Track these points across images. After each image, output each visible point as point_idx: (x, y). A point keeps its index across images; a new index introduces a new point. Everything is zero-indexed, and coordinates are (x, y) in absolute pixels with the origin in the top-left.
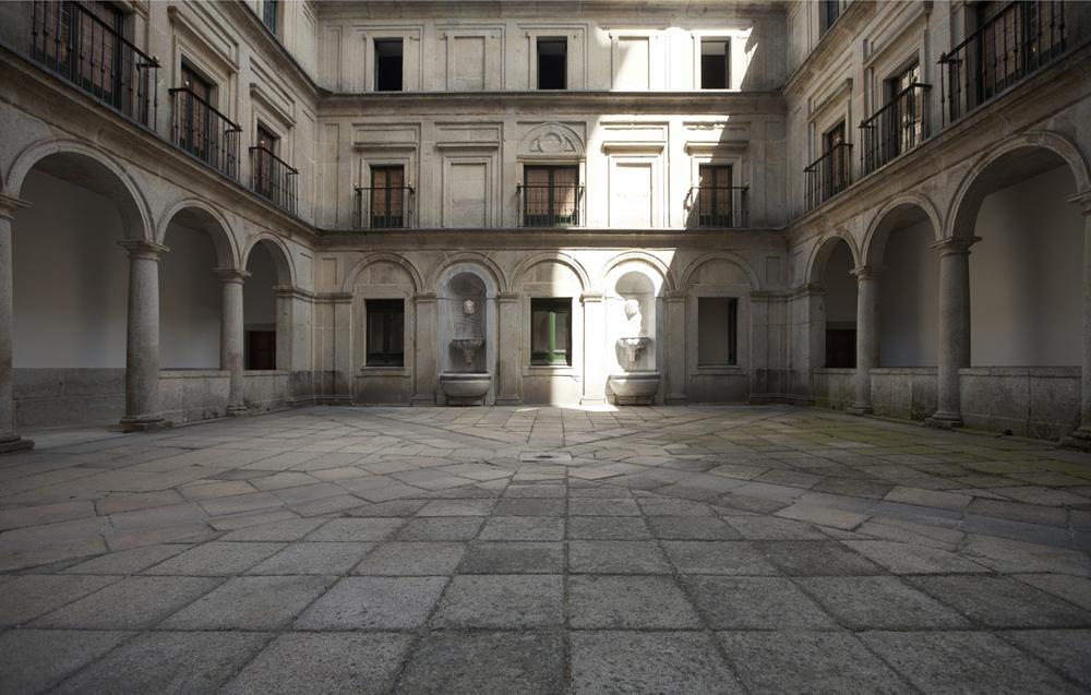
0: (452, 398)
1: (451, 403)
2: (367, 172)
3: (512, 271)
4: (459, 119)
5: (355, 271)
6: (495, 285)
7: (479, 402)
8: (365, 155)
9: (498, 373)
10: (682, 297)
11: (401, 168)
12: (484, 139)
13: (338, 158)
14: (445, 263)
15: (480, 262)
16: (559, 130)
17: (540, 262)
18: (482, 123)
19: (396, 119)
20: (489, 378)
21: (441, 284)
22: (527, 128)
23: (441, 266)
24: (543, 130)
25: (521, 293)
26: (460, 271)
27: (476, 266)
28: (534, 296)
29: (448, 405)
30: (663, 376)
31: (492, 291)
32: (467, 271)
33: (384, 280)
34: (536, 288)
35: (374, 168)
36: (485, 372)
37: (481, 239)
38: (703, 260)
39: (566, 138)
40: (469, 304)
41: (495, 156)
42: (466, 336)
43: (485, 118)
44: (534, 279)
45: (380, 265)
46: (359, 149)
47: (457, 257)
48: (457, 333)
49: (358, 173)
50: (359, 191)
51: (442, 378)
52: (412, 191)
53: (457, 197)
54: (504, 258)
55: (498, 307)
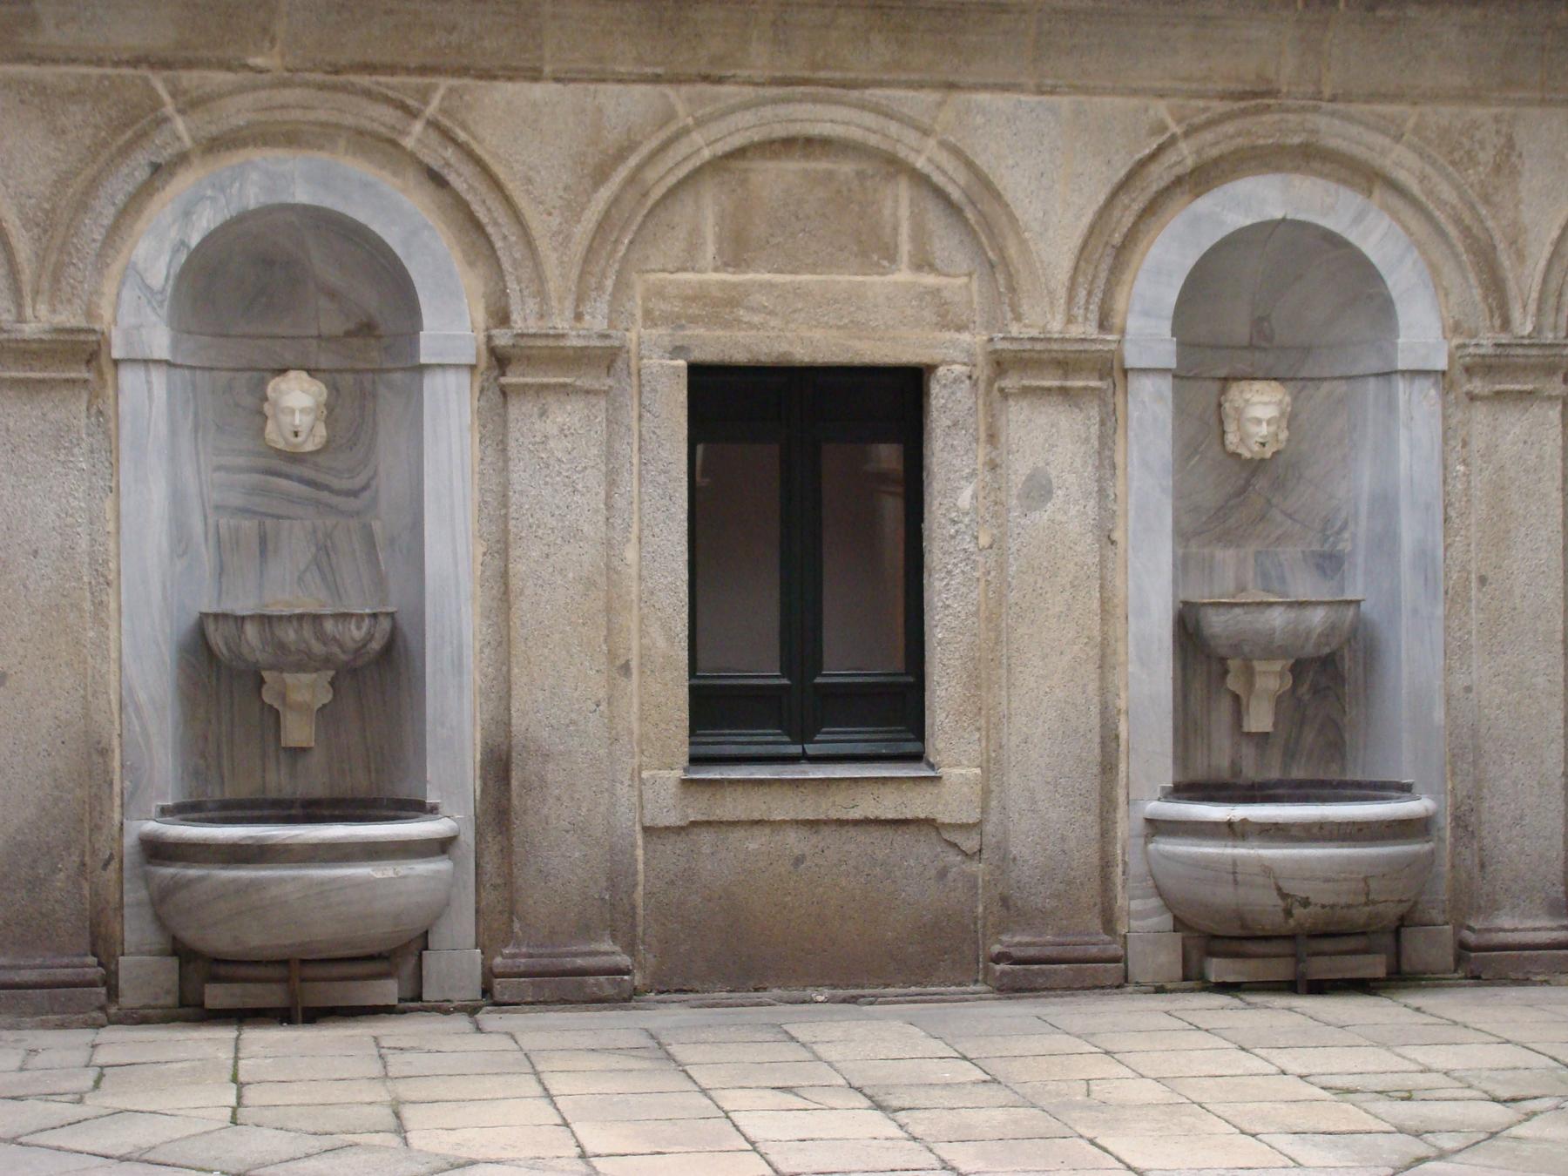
0: (219, 966)
1: (216, 995)
3: (573, 211)
7: (388, 991)
14: (160, 147)
15: (384, 148)
17: (740, 153)
20: (442, 846)
23: (136, 169)
25: (635, 335)
26: (252, 195)
28: (700, 356)
30: (1446, 822)
31: (450, 324)
32: (302, 195)
36: (417, 808)
40: (298, 399)
42: (285, 589)
44: (711, 249)
47: (238, 112)
48: (221, 570)
51: (157, 851)
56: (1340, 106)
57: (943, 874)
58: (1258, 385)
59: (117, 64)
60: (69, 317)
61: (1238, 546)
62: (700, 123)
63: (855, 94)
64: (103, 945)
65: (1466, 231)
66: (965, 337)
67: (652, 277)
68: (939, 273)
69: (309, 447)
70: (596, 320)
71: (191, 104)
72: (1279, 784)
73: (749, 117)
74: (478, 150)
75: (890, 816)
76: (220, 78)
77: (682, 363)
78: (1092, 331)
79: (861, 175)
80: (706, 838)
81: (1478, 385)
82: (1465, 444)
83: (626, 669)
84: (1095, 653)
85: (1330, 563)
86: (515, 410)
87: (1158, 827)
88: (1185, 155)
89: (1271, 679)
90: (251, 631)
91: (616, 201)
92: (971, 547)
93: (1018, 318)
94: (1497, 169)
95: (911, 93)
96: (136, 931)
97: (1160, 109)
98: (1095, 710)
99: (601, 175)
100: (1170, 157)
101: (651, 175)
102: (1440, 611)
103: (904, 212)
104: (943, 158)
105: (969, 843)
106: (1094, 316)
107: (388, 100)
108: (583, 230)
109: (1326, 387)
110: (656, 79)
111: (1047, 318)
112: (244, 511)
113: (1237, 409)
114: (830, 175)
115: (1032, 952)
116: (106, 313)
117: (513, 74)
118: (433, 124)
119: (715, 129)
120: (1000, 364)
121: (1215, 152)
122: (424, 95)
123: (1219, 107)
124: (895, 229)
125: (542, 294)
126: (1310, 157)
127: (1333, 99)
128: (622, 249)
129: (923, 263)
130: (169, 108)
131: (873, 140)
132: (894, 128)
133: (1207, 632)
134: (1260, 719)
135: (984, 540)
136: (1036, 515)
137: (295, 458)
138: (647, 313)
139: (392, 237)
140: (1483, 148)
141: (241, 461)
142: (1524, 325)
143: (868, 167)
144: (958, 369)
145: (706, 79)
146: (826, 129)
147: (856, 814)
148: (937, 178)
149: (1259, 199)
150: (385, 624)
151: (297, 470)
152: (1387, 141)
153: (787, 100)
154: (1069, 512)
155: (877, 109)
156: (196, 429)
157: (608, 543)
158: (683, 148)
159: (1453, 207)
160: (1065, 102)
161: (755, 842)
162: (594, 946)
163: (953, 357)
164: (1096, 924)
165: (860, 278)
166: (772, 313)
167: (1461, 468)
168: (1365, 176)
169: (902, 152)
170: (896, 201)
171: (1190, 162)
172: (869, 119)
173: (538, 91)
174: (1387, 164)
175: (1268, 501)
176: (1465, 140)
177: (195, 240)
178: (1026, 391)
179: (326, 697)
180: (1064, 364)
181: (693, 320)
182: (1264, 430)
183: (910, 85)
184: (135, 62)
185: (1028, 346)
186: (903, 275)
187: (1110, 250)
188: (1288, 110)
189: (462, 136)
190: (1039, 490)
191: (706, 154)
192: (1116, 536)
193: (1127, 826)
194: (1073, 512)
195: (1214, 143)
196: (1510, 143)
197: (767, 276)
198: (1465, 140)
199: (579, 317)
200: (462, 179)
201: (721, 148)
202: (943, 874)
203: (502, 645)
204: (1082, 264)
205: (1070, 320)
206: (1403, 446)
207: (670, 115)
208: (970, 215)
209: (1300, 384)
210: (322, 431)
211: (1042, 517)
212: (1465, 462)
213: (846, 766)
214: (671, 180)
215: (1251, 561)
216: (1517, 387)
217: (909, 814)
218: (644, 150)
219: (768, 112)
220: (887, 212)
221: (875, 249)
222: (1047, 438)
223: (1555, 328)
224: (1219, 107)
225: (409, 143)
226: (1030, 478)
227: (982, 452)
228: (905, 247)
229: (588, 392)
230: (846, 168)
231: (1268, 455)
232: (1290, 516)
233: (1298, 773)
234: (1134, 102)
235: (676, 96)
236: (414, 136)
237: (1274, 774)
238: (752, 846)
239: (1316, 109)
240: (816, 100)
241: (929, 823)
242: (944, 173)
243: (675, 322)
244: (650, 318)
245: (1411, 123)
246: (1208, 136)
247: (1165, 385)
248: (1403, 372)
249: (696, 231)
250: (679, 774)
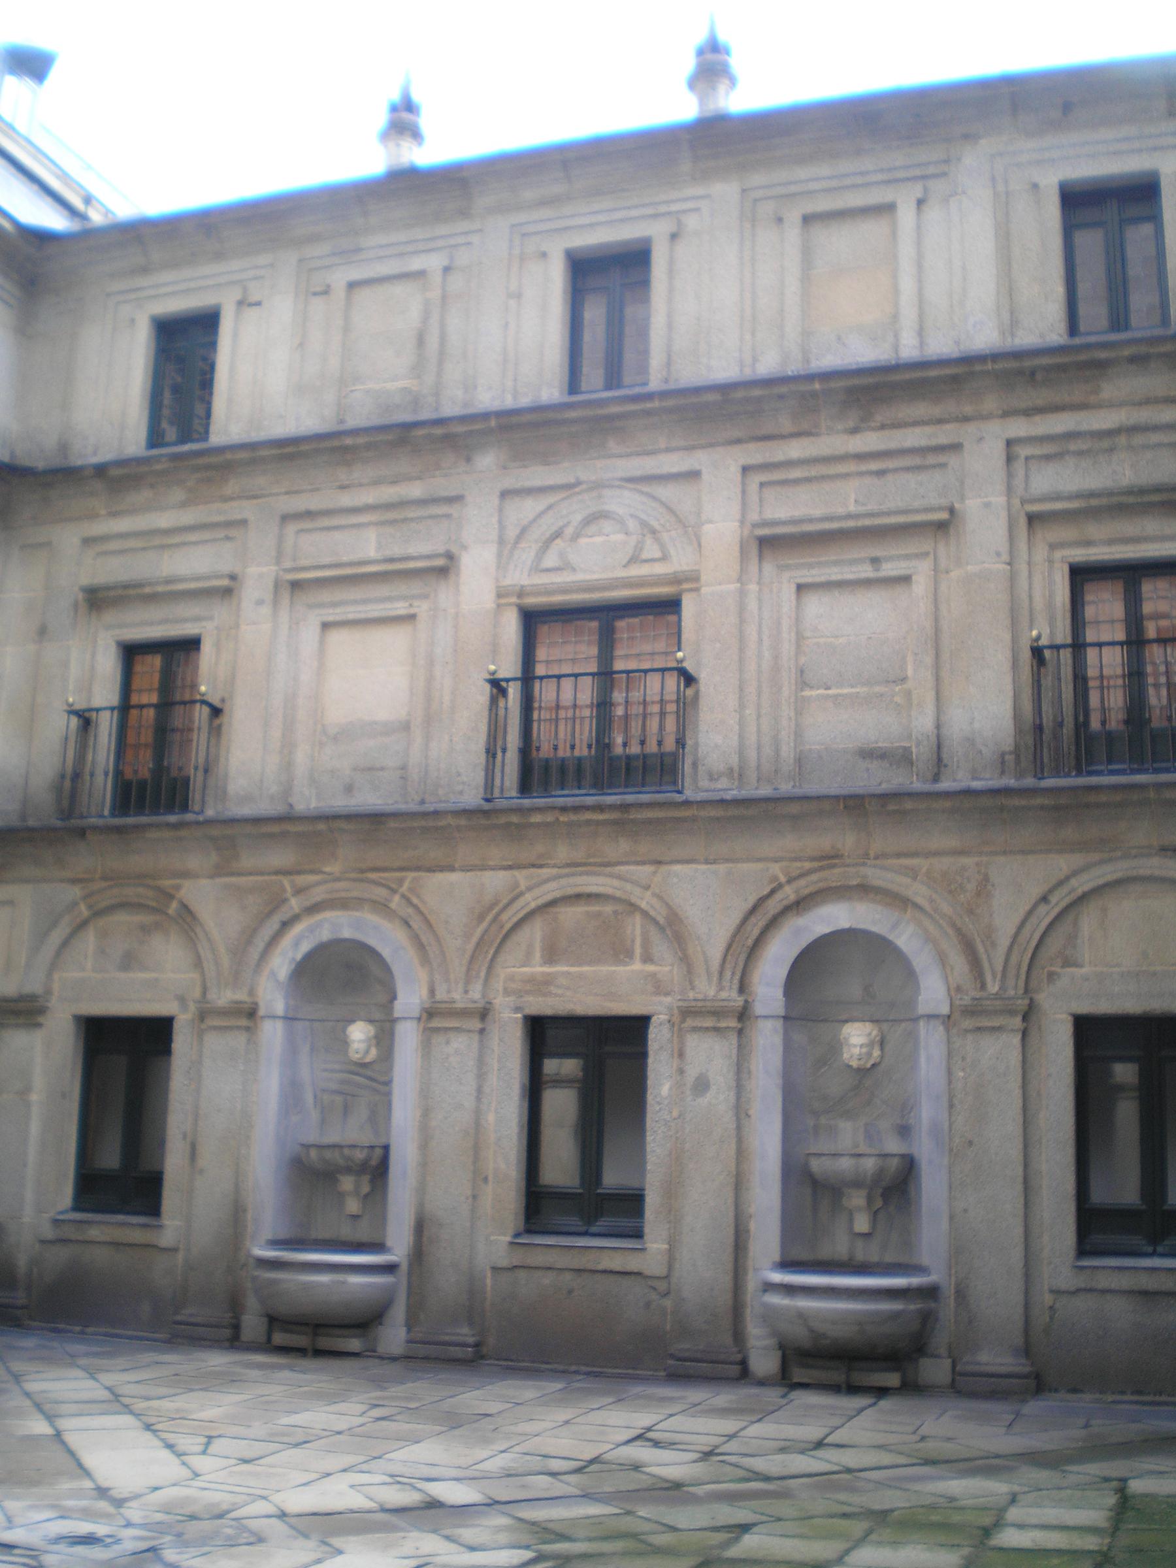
2: (108, 664)
4: (346, 500)
5: (56, 937)
6: (422, 975)
7: (354, 1344)
8: (110, 616)
9: (418, 1254)
10: (1012, 1013)
11: (192, 644)
12: (412, 550)
13: (42, 632)
15: (381, 907)
16: (623, 502)
17: (553, 903)
18: (402, 504)
19: (188, 517)
20: (390, 1268)
21: (273, 974)
22: (530, 507)
23: (273, 924)
24: (574, 510)
26: (325, 935)
27: (371, 918)
29: (268, 1347)
31: (410, 998)
32: (347, 933)
33: (128, 962)
34: (542, 985)
35: (131, 652)
36: (377, 1247)
37: (383, 835)
38: (1082, 884)
39: (644, 524)
40: (359, 1033)
41: (444, 595)
42: (353, 1132)
43: (415, 490)
44: (538, 955)
45: (122, 918)
46: (97, 599)
47: (318, 894)
48: (323, 1122)
49: (91, 671)
50: (86, 720)
51: (264, 1263)
52: (216, 712)
53: (337, 714)
54: (452, 894)
55: (426, 1047)
56: (878, 862)
57: (648, 1305)
59: (269, 874)
60: (241, 996)
62: (529, 889)
63: (609, 869)
64: (235, 1305)
65: (959, 931)
66: (669, 999)
67: (509, 970)
68: (657, 965)
69: (367, 1060)
70: (476, 992)
71: (298, 891)
72: (878, 1265)
73: (552, 885)
74: (423, 909)
75: (618, 1269)
76: (312, 878)
77: (519, 1015)
78: (734, 994)
79: (615, 912)
80: (522, 1274)
81: (968, 1023)
82: (964, 1059)
83: (486, 1180)
84: (733, 1179)
85: (904, 1131)
86: (438, 1039)
87: (769, 1287)
88: (789, 893)
89: (857, 1199)
90: (313, 1153)
91: (486, 931)
92: (668, 1117)
93: (693, 988)
94: (978, 894)
95: (640, 868)
96: (252, 1303)
97: (776, 869)
98: (731, 1214)
99: (481, 918)
100: (779, 896)
101: (504, 917)
102: (946, 1161)
103: (638, 932)
104: (654, 901)
105: (662, 1286)
106: (736, 986)
107: (384, 885)
108: (470, 946)
109: (903, 1025)
110: (510, 868)
111: (706, 989)
112: (339, 1092)
114: (599, 914)
115: (687, 1354)
116: (260, 992)
117: (442, 869)
118: (403, 896)
119: (537, 892)
120: (687, 1012)
121: (806, 892)
122: (401, 881)
123: (807, 865)
124: (633, 941)
125: (447, 980)
126: (865, 890)
127: (876, 858)
128: (490, 956)
129: (647, 958)
130: (288, 895)
131: (618, 894)
132: (628, 887)
134: (862, 1224)
135: (675, 1114)
136: (700, 1100)
137: (364, 1065)
138: (505, 989)
139: (386, 953)
140: (969, 881)
141: (337, 1067)
142: (993, 987)
143: (619, 908)
144: (662, 1017)
145: (534, 866)
146: (593, 889)
147: (600, 1267)
148: (652, 913)
149: (834, 916)
150: (379, 1152)
151: (361, 1071)
152: (909, 880)
153: (573, 875)
154: (719, 1098)
155: (619, 877)
156: (312, 1049)
157: (478, 1113)
158: (521, 902)
159: (950, 918)
160: (722, 868)
161: (547, 1279)
162: (458, 1331)
163: (660, 1011)
164: (728, 1339)
165: (614, 968)
166: (568, 988)
167: (961, 1074)
168: (898, 901)
169: (634, 900)
170: (634, 925)
171: (793, 897)
172: (616, 883)
173: (454, 877)
174: (909, 893)
176: (958, 878)
177: (299, 957)
178: (695, 1029)
179: (366, 1189)
180: (717, 1013)
181: (528, 992)
182: (857, 1051)
183: (638, 863)
184: (278, 872)
185: (693, 1004)
186: (637, 966)
187: (746, 950)
188: (848, 866)
189: (415, 901)
190: (702, 1085)
191: (533, 905)
192: (751, 1112)
193: (751, 1284)
194: (722, 1097)
195: (805, 886)
196: (986, 878)
197: (565, 969)
198: (958, 878)
199: (466, 992)
200: (416, 923)
201: (540, 902)
202: (648, 1305)
203: (424, 1165)
204: (729, 957)
205: (721, 988)
206: (923, 1060)
207: (517, 885)
208: (669, 932)
210: (374, 1052)
211: (704, 1101)
212: (963, 1070)
213: (619, 1240)
214: (515, 919)
216: (990, 1024)
217: (629, 1268)
218: (501, 905)
219: (563, 881)
220: (629, 932)
221: (621, 953)
222: (709, 1055)
223: (1016, 987)
224: (807, 865)
225: (393, 905)
226: (697, 1079)
227: (676, 1062)
228: (638, 951)
229: (469, 1031)
230: (608, 909)
231: (869, 1066)
233: (889, 1258)
234: (760, 865)
235: (521, 876)
236: (396, 902)
237: (875, 1258)
238: (546, 1281)
239: (864, 864)
240: (587, 873)
241: (639, 1274)
242: (655, 910)
243: (519, 994)
244: (507, 992)
245: (924, 870)
246: (802, 882)
247: (779, 1024)
248: (923, 1016)
249: (530, 946)
250: (508, 1239)
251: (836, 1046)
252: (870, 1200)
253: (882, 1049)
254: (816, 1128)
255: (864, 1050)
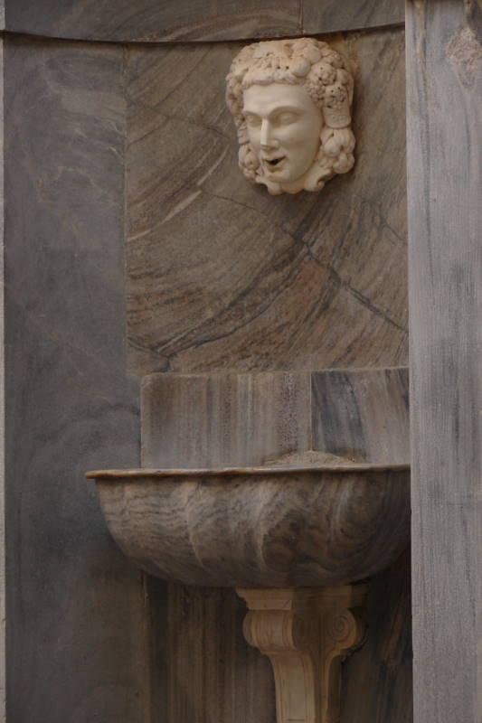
58: (262, 49)
61: (281, 365)
113: (234, 98)
133: (111, 531)
175: (334, 274)
182: (260, 134)
206: (413, 150)
209: (381, 39)
215: (307, 394)
231: (312, 183)
232: (367, 303)
251: (219, 125)
252: (311, 631)
253: (355, 127)
254: (162, 397)
255: (284, 132)
